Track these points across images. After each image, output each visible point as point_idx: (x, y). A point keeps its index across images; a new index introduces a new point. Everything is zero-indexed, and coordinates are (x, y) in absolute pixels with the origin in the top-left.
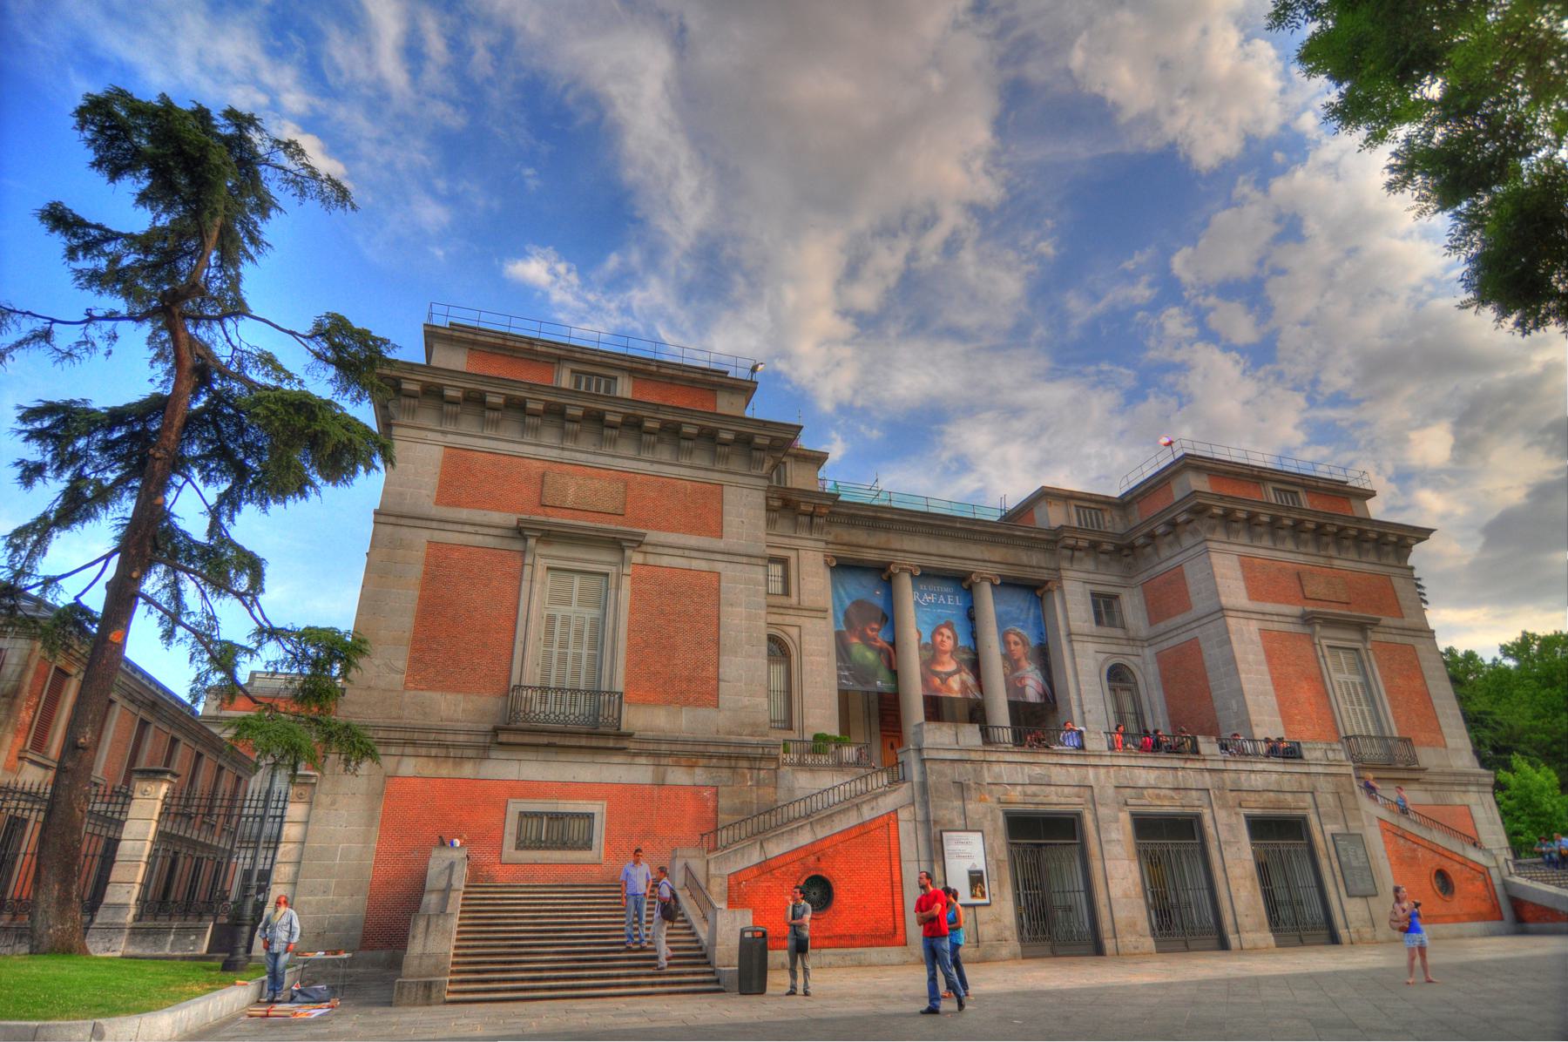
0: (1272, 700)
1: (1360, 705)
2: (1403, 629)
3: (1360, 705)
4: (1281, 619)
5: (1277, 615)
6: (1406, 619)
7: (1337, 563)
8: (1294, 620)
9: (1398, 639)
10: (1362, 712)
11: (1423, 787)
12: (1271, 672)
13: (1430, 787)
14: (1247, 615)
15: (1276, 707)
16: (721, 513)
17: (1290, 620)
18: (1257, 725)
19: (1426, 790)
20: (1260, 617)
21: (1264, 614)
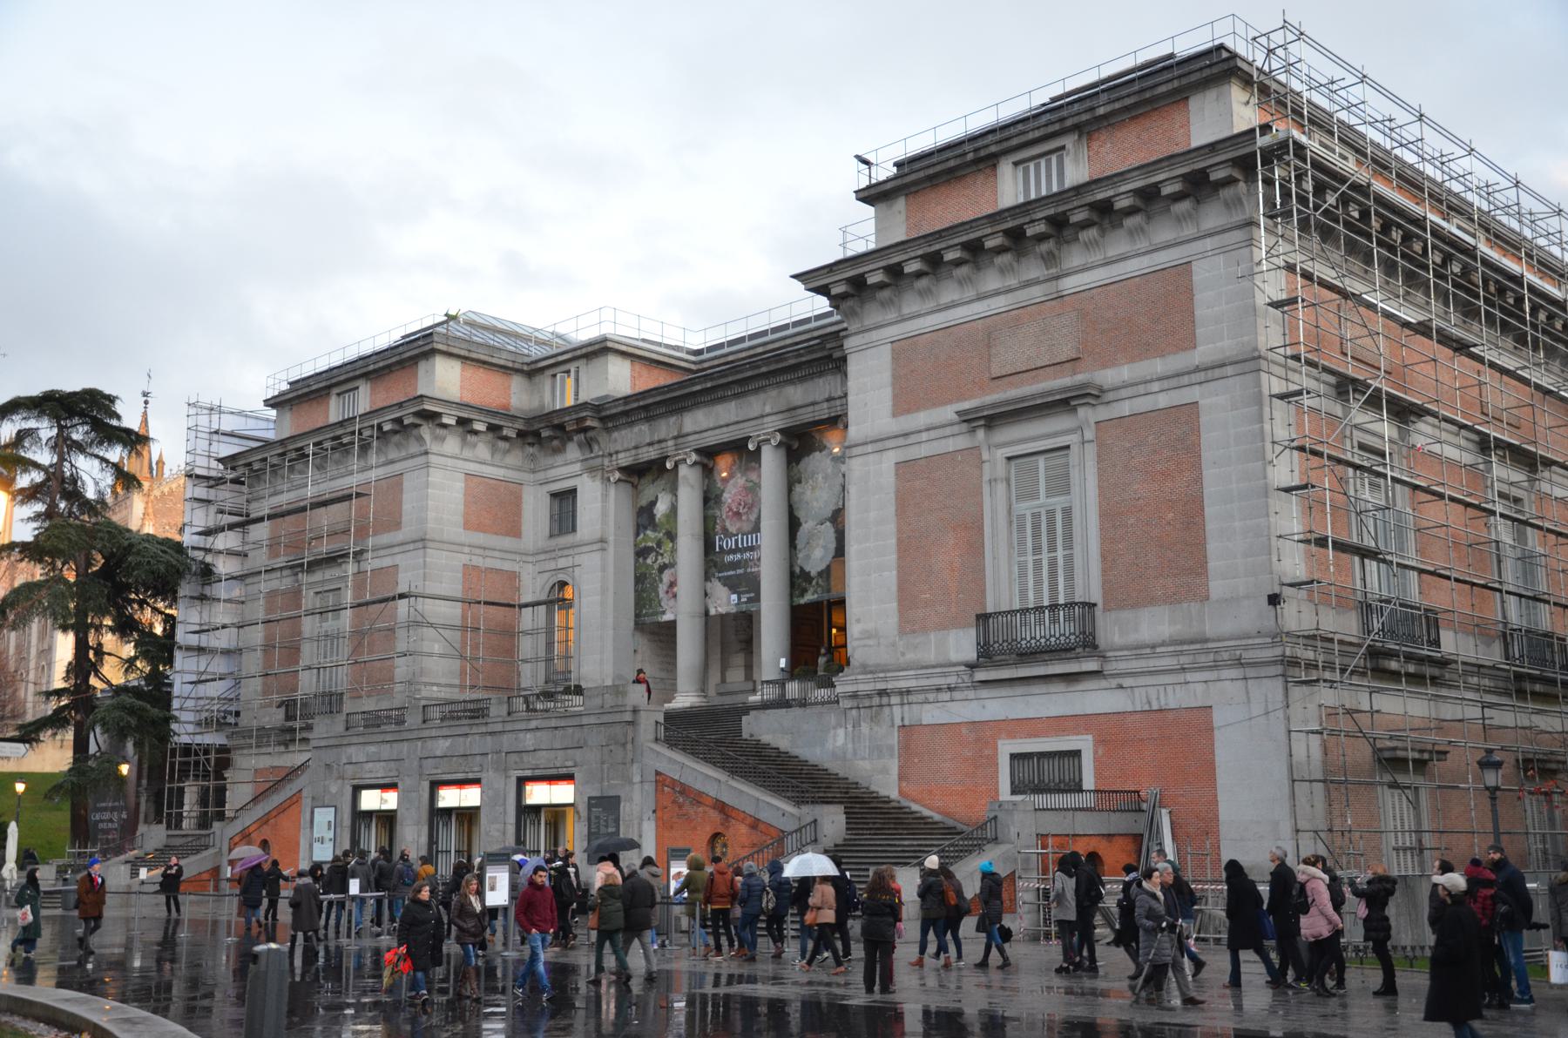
0: (891, 577)
1: (1052, 548)
2: (1197, 369)
3: (1052, 548)
4: (933, 434)
5: (928, 430)
6: (1200, 349)
7: (1070, 284)
8: (956, 429)
9: (1163, 401)
10: (1053, 564)
11: (1114, 682)
12: (899, 531)
13: (1127, 682)
14: (879, 446)
15: (894, 588)
16: (400, 503)
17: (948, 431)
18: (858, 621)
19: (1121, 687)
20: (901, 441)
21: (906, 435)
